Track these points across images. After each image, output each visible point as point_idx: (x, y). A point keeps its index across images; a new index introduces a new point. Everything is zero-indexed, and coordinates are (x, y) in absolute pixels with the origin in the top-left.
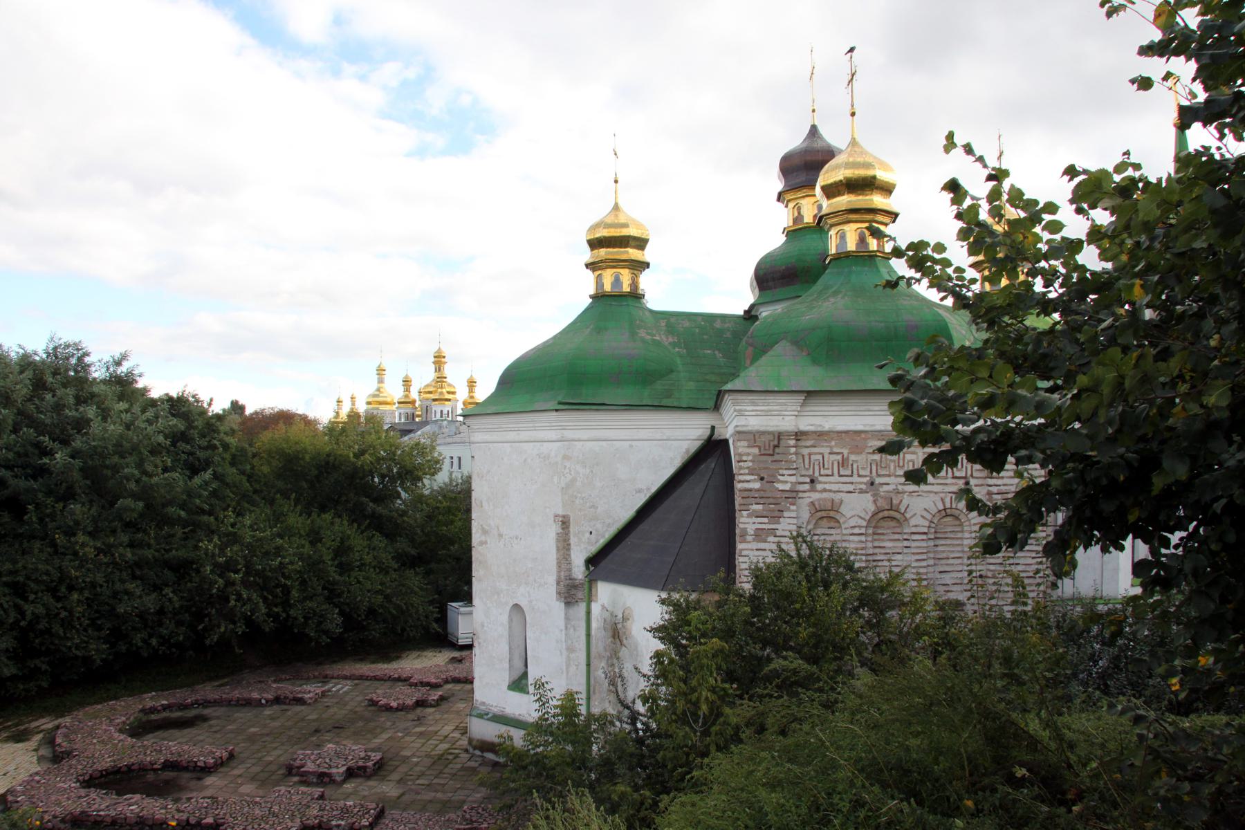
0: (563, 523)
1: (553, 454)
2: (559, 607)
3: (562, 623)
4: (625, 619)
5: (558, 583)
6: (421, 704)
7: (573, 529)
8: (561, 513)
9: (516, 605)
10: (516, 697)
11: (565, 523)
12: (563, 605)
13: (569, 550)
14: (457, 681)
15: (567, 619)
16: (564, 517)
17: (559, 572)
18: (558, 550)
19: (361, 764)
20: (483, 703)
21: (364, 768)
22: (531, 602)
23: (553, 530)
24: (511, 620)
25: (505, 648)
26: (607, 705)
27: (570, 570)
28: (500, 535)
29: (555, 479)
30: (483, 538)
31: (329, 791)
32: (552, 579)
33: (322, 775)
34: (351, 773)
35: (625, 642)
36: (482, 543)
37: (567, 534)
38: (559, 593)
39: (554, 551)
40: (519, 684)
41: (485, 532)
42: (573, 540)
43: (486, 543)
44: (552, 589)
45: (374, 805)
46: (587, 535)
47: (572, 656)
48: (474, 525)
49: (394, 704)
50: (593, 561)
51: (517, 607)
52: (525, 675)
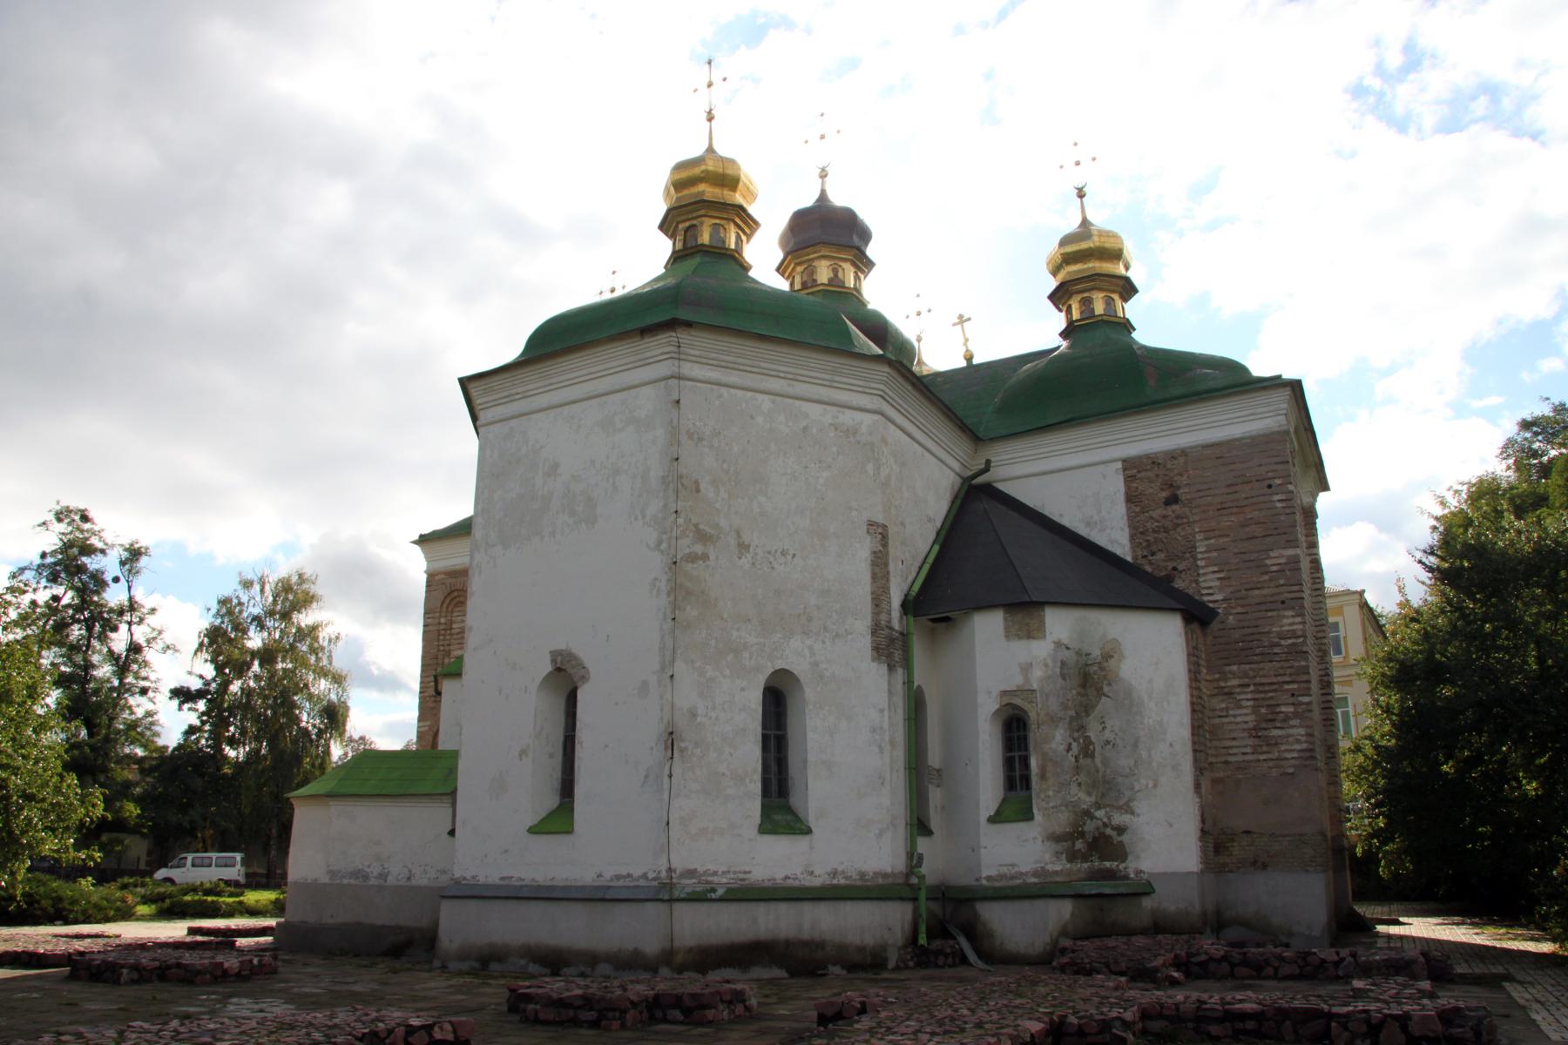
1: (864, 429)
4: (1107, 657)
5: (874, 633)
8: (880, 519)
12: (884, 667)
20: (691, 873)
22: (816, 664)
23: (863, 550)
26: (1074, 789)
28: (743, 547)
29: (870, 468)
30: (699, 549)
32: (861, 626)
35: (1106, 689)
38: (876, 649)
39: (867, 578)
43: (705, 557)
44: (865, 643)
50: (911, 606)
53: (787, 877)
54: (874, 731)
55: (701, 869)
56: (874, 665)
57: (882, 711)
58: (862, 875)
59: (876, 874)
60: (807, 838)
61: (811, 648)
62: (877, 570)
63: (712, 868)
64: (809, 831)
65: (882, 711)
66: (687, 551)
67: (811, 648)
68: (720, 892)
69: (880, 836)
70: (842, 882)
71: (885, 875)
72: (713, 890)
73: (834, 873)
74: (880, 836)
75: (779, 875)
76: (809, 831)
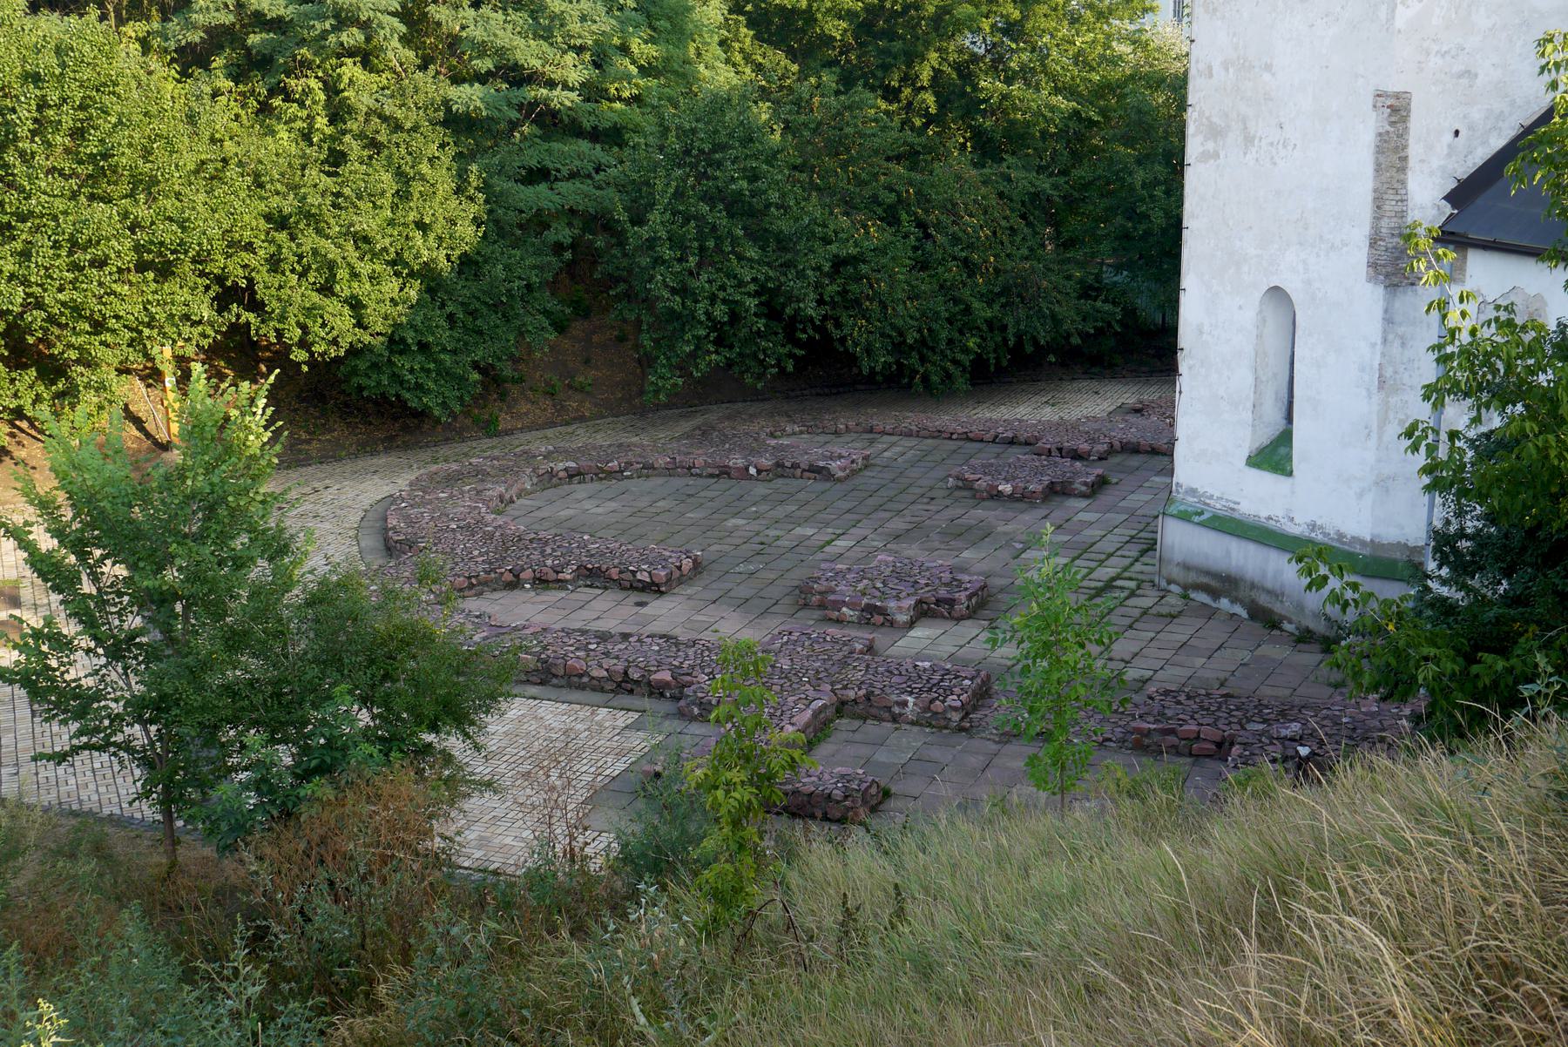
0: (1394, 110)
2: (1371, 297)
3: (1374, 328)
5: (1373, 243)
6: (1057, 491)
7: (1416, 124)
9: (1276, 289)
10: (1266, 482)
11: (1397, 110)
12: (1380, 290)
13: (1403, 170)
14: (1132, 449)
15: (1389, 320)
16: (1397, 96)
17: (1377, 219)
18: (1378, 169)
19: (943, 592)
20: (1192, 492)
21: (951, 602)
23: (1367, 128)
24: (1262, 321)
25: (1243, 378)
27: (1402, 214)
28: (1249, 140)
30: (1210, 146)
31: (881, 638)
32: (1359, 234)
33: (871, 609)
34: (1112, 451)
36: (1205, 157)
37: (1402, 135)
38: (1373, 265)
40: (1274, 456)
41: (1215, 133)
42: (1415, 150)
43: (1216, 156)
44: (1359, 256)
45: (970, 672)
46: (1450, 136)
47: (1393, 400)
48: (1192, 118)
49: (1006, 488)
51: (1277, 293)
52: (1285, 438)
53: (1270, 518)
54: (1363, 370)
55: (1201, 491)
56: (1370, 286)
57: (1374, 345)
58: (1341, 536)
59: (1355, 540)
60: (1288, 481)
61: (1304, 262)
62: (1382, 159)
63: (1210, 491)
64: (1290, 474)
65: (1374, 345)
66: (1201, 149)
67: (1304, 262)
68: (1206, 516)
69: (1360, 495)
70: (1320, 537)
71: (1363, 543)
72: (1201, 513)
73: (1313, 526)
74: (1360, 495)
75: (1264, 514)
76: (1290, 474)
